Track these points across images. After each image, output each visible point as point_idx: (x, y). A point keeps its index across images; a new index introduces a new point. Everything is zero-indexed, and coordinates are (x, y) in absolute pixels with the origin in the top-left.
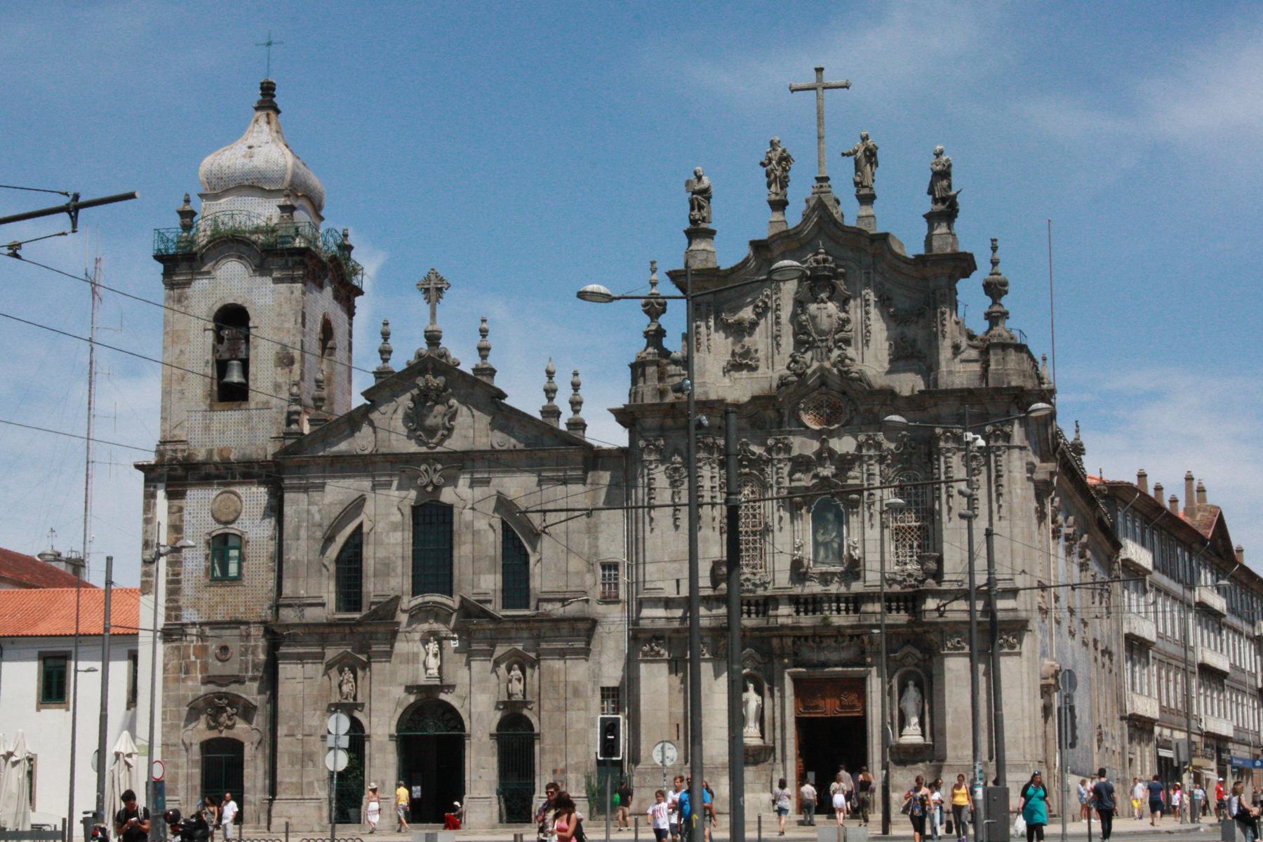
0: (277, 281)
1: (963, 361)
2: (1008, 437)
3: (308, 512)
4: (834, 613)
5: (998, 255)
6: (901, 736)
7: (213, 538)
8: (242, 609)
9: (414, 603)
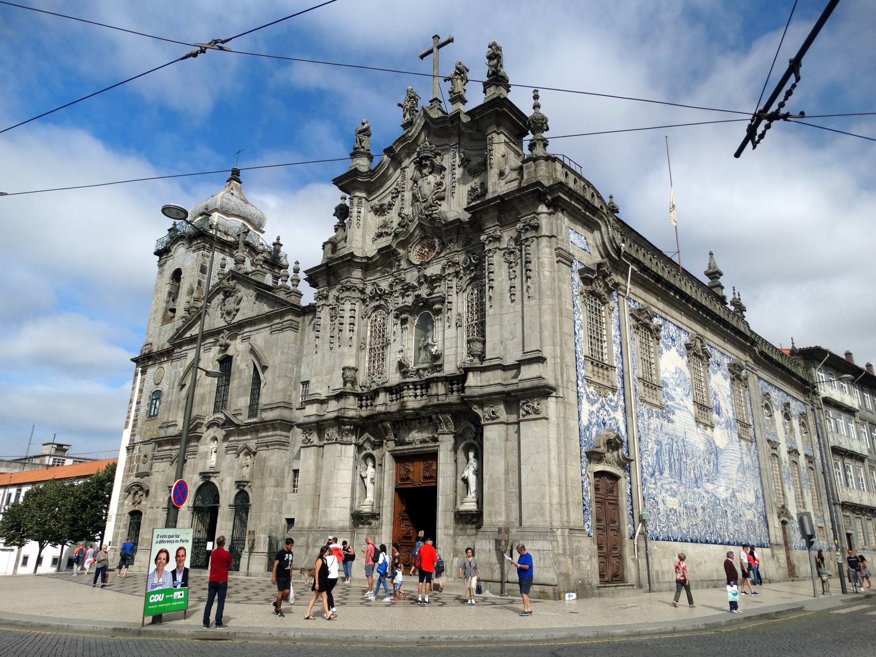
0: (194, 251)
1: (506, 183)
2: (536, 228)
3: (180, 373)
4: (412, 398)
5: (540, 101)
6: (462, 503)
7: (153, 393)
8: (155, 433)
9: (210, 420)
